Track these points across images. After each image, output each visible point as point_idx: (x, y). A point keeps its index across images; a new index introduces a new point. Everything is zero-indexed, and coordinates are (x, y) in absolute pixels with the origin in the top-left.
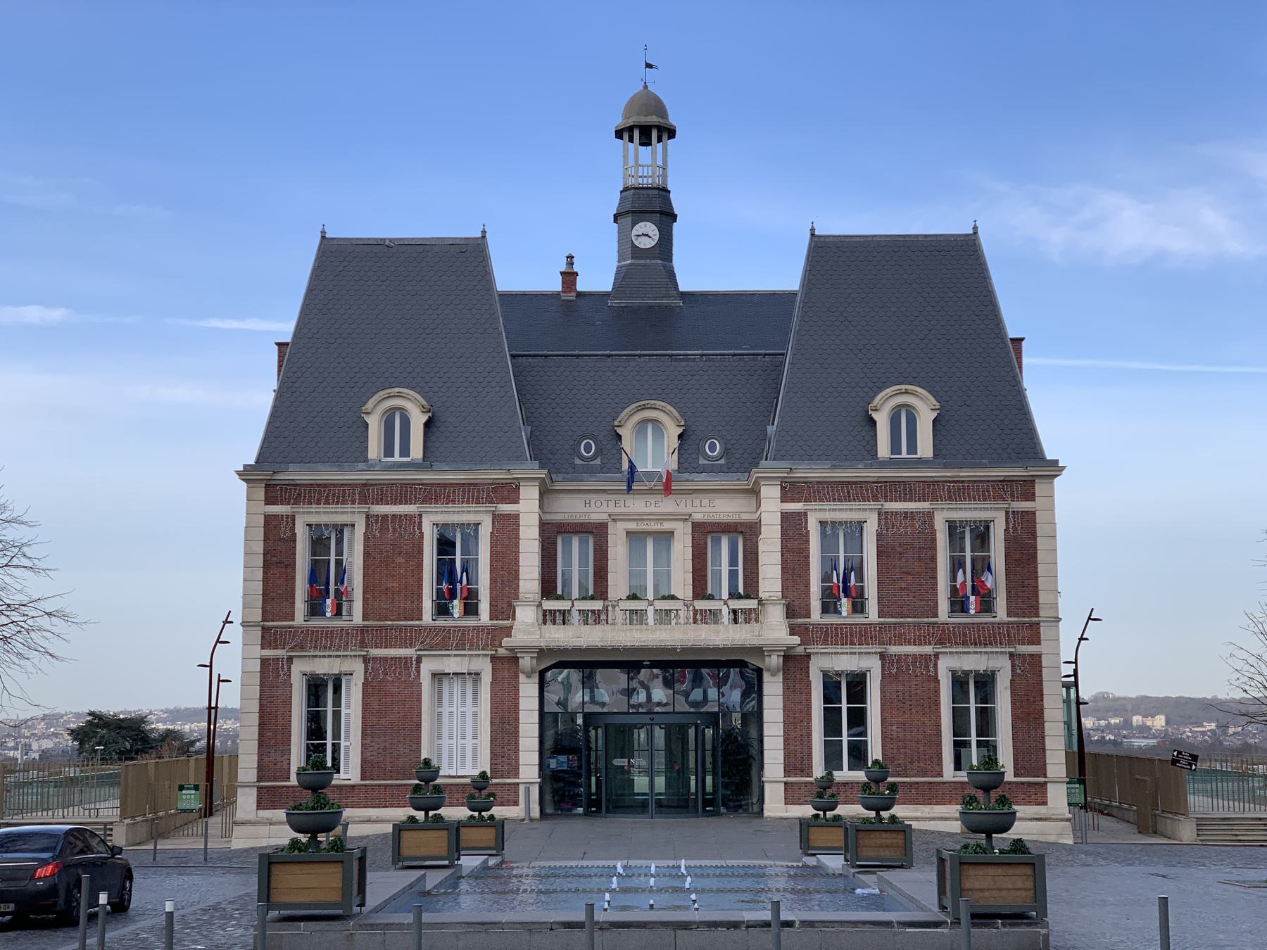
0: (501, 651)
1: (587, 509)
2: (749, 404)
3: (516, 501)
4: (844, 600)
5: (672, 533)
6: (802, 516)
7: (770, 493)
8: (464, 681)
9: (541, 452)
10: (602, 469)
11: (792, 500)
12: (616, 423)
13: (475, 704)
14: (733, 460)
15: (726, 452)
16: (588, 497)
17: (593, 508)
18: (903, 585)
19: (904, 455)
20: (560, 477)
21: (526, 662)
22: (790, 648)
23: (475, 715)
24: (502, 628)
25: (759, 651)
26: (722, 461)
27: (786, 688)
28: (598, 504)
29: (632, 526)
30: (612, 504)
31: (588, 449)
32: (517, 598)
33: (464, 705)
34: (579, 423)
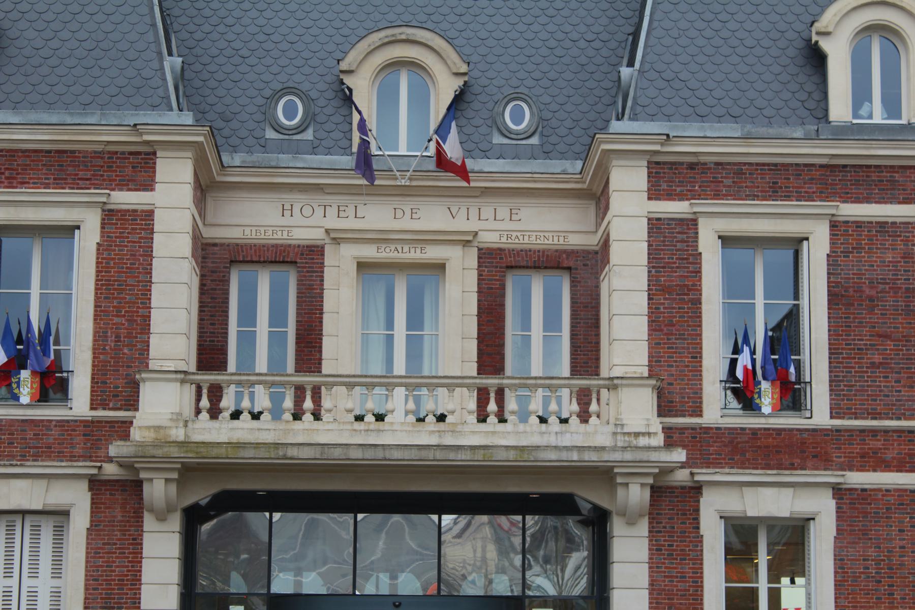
0: (111, 470)
1: (287, 221)
2: (582, 44)
3: (148, 185)
4: (765, 386)
5: (441, 267)
6: (688, 227)
7: (629, 185)
8: (36, 529)
9: (190, 90)
10: (314, 150)
11: (670, 196)
12: (344, 66)
13: (57, 573)
14: (554, 139)
15: (541, 126)
16: (288, 197)
17: (297, 219)
18: (877, 359)
19: (878, 118)
20: (237, 159)
21: (157, 490)
22: (667, 470)
23: (56, 595)
24: (111, 423)
25: (605, 475)
26: (535, 140)
27: (655, 549)
28: (307, 211)
29: (369, 252)
30: (332, 212)
31: (288, 112)
32: (145, 367)
33: (34, 574)
34: (275, 69)
